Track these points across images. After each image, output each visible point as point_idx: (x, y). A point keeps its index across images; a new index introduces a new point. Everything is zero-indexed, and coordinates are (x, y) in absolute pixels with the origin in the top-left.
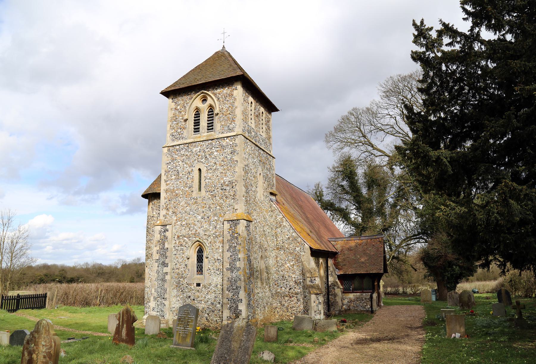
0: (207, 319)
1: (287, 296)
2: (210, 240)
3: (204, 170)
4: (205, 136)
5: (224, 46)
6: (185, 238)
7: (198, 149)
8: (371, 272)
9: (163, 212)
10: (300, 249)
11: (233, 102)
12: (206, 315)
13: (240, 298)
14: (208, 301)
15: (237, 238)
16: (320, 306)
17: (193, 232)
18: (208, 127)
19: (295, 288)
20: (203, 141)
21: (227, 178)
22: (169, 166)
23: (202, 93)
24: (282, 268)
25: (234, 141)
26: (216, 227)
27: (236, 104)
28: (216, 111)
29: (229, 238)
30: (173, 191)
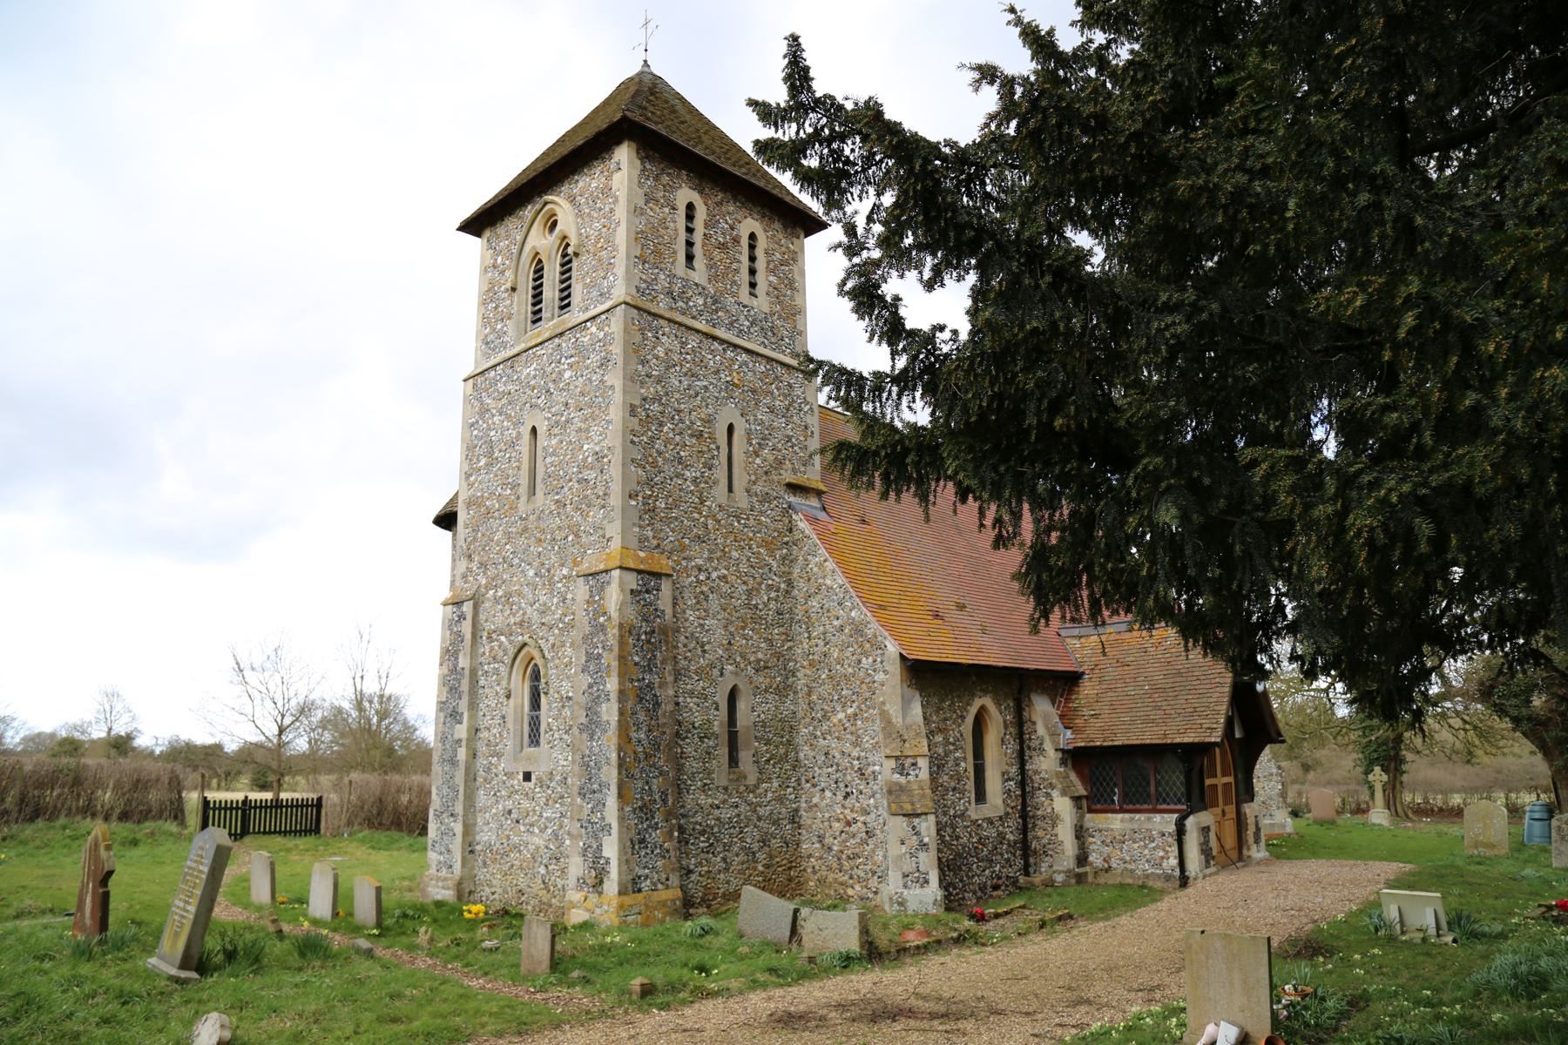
0: (544, 882)
1: (838, 820)
2: (551, 639)
3: (541, 431)
4: (549, 328)
5: (645, 61)
6: (503, 638)
7: (531, 370)
8: (1178, 740)
10: (875, 661)
11: (612, 211)
12: (542, 870)
13: (607, 822)
14: (546, 828)
16: (922, 856)
19: (861, 793)
20: (541, 343)
21: (591, 446)
22: (475, 432)
23: (546, 203)
24: (825, 727)
25: (606, 329)
29: (588, 629)
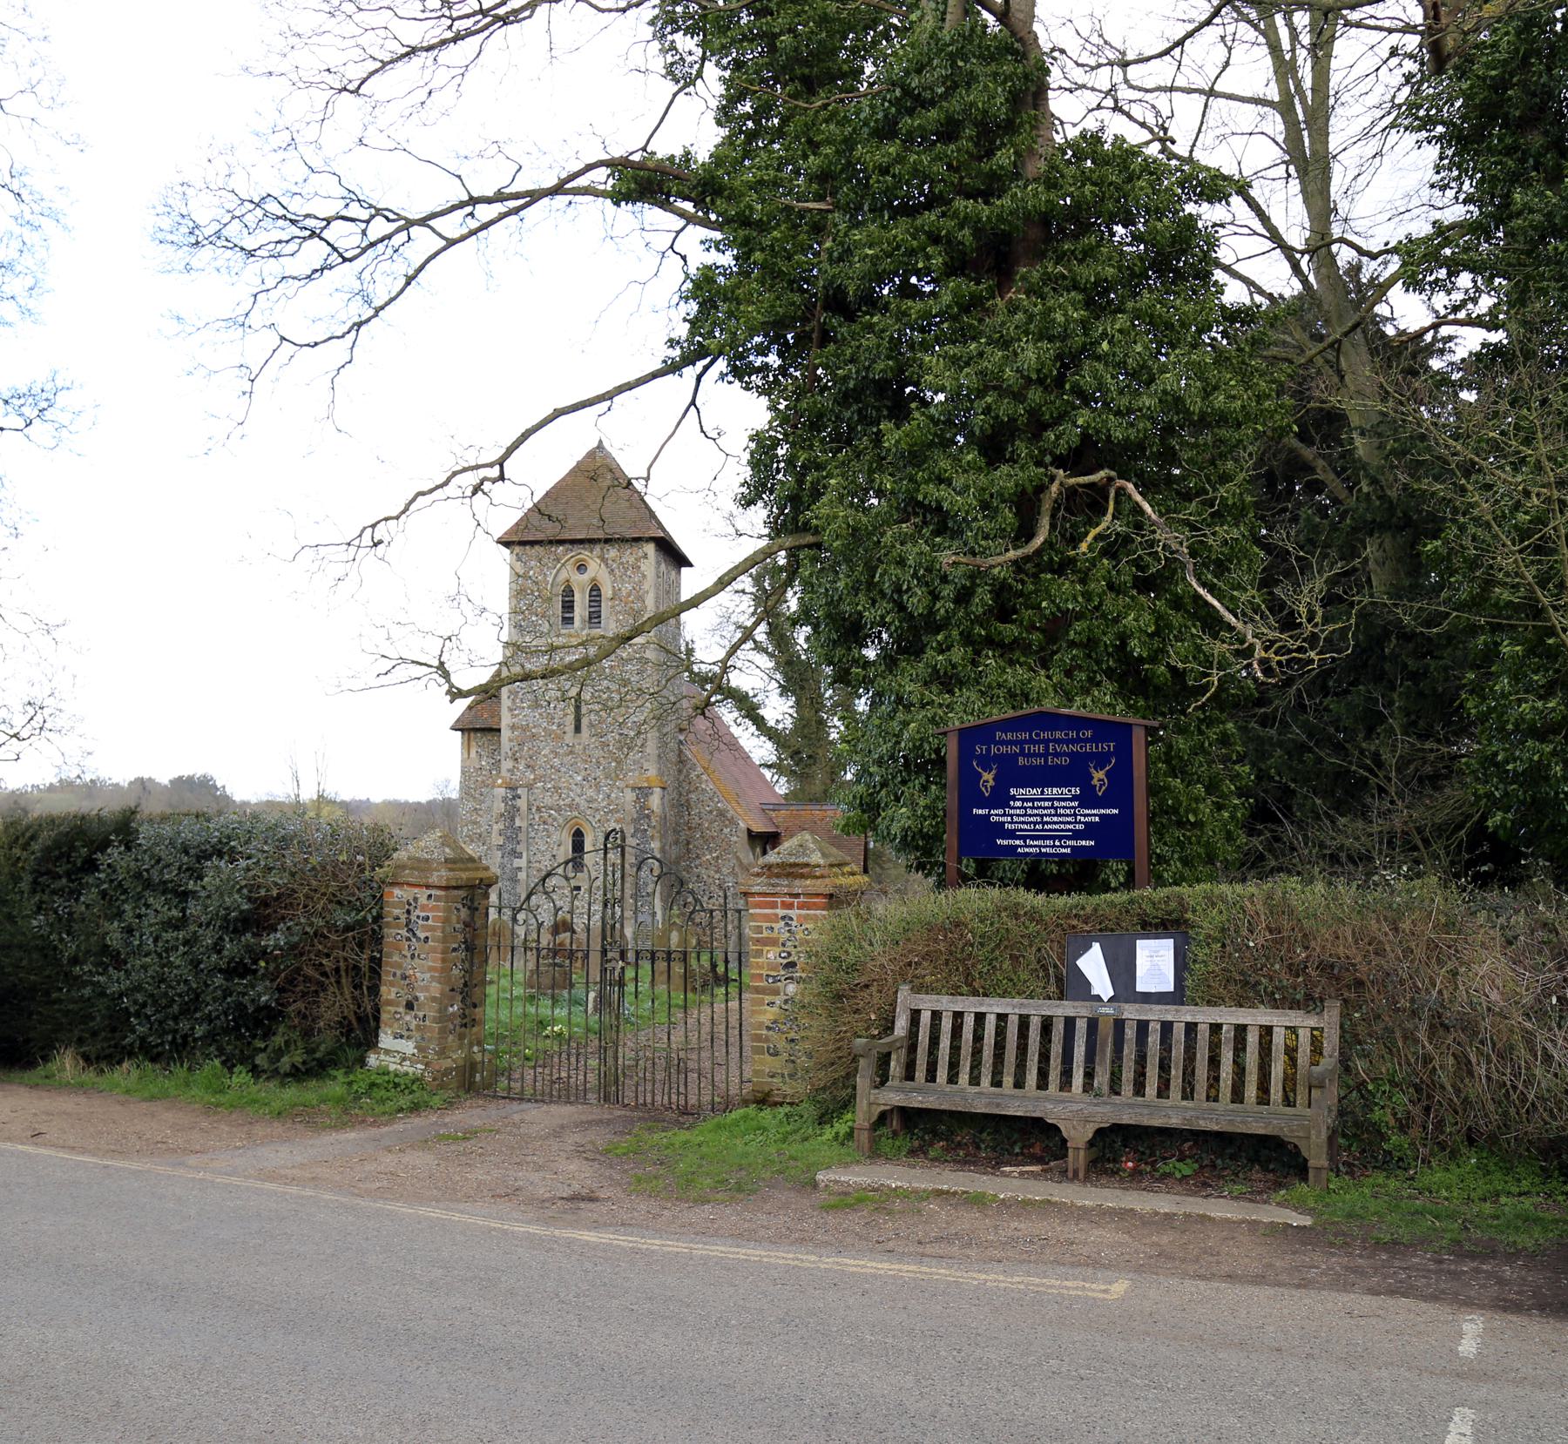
2: (598, 817)
9: (507, 765)
15: (648, 816)
17: (568, 801)
18: (590, 618)
26: (609, 796)
27: (646, 586)
28: (607, 592)
30: (525, 729)
